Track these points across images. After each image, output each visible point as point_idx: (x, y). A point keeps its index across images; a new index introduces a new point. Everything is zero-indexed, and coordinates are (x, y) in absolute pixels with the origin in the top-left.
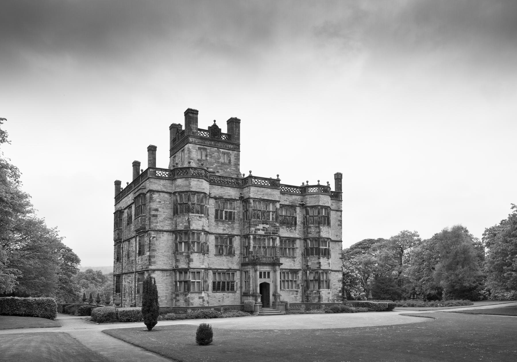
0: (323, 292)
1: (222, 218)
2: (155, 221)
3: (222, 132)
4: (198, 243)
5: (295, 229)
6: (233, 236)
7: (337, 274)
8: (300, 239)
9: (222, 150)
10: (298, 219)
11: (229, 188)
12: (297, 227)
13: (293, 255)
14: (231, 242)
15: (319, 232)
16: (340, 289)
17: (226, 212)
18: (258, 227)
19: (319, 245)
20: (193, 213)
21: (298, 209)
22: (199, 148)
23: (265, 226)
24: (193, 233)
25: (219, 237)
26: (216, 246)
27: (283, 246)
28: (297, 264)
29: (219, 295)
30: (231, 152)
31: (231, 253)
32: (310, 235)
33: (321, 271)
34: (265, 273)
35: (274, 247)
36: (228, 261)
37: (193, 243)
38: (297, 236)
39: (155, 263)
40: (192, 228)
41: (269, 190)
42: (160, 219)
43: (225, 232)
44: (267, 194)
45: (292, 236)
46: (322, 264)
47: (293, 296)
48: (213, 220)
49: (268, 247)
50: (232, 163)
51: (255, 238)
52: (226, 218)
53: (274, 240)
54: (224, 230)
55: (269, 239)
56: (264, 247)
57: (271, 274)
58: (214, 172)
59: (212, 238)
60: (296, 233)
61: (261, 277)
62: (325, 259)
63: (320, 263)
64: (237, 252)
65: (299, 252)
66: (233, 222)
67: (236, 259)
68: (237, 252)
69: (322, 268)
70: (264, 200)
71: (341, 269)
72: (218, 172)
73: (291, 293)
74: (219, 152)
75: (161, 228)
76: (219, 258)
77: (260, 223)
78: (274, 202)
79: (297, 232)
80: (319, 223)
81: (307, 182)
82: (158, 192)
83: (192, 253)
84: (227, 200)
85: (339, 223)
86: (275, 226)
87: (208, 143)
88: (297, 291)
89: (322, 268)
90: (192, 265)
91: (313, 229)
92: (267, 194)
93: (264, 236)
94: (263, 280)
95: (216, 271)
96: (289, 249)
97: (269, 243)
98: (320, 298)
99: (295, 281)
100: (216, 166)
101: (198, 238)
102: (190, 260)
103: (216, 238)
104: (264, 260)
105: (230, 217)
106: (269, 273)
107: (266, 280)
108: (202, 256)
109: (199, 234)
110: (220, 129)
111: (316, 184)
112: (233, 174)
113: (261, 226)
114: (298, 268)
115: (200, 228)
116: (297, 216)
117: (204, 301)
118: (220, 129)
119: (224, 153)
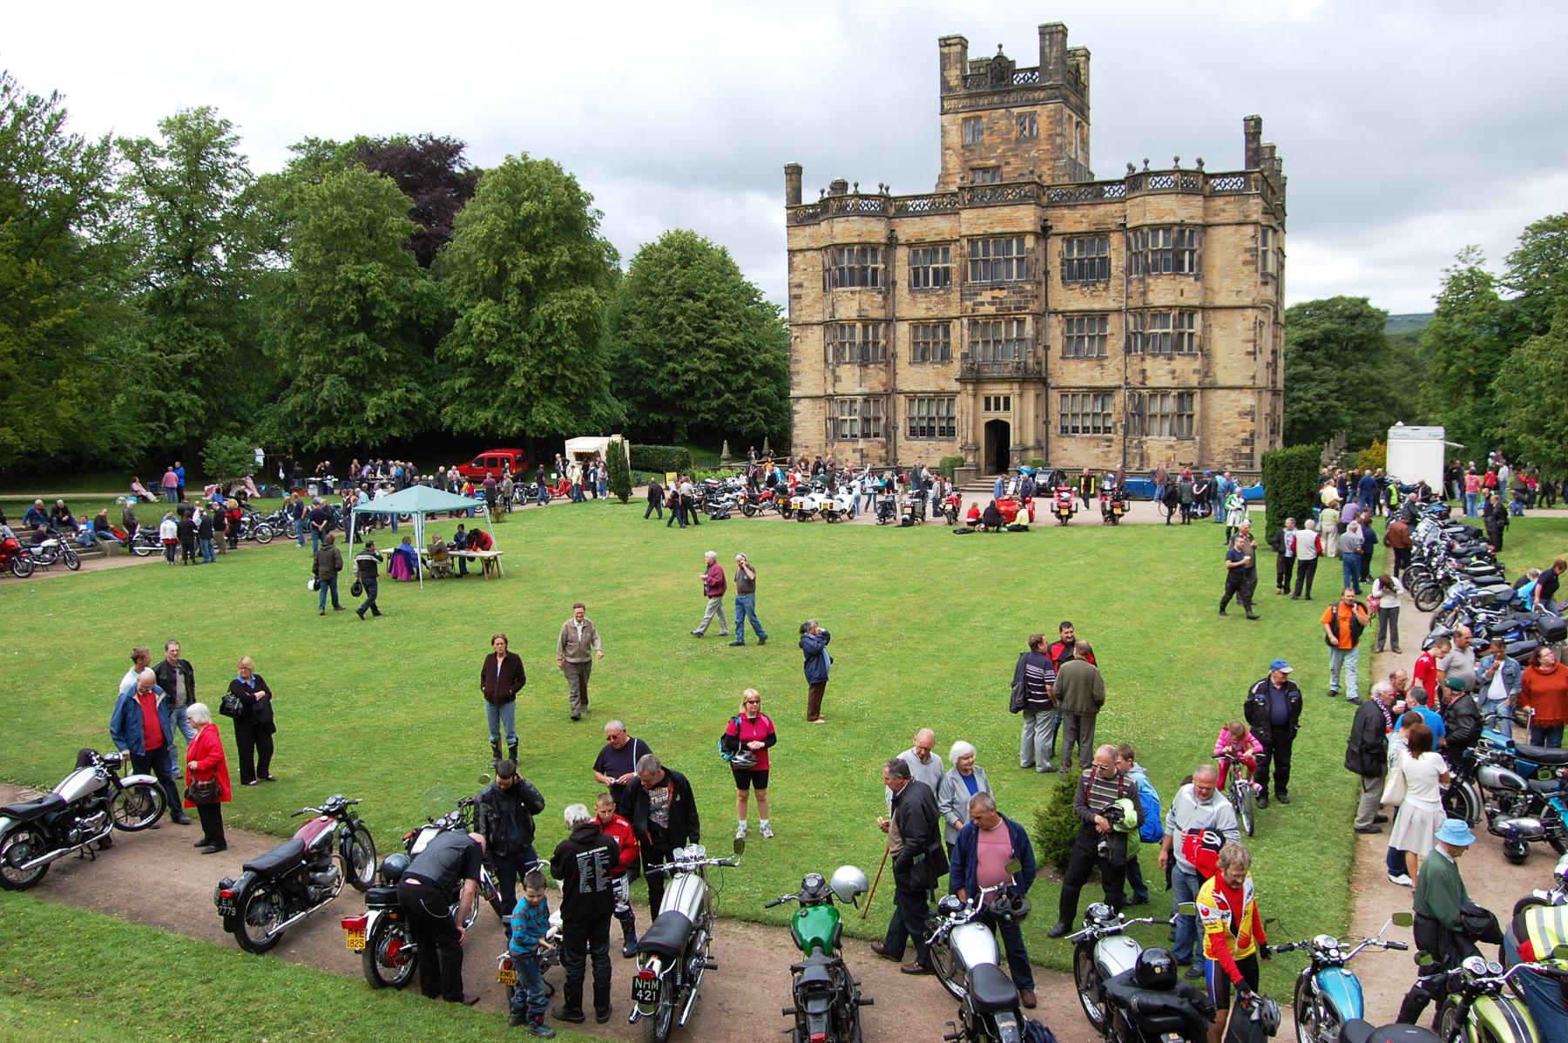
0: (1150, 443)
1: (926, 283)
2: (797, 307)
3: (1018, 67)
4: (852, 344)
5: (1106, 289)
6: (950, 319)
7: (1234, 395)
8: (1119, 311)
9: (1016, 111)
10: (1113, 263)
11: (937, 218)
12: (1112, 283)
13: (1101, 350)
14: (947, 333)
15: (1144, 294)
16: (1246, 435)
17: (936, 271)
18: (979, 299)
19: (1143, 327)
20: (842, 285)
21: (1116, 240)
22: (965, 120)
23: (996, 293)
24: (842, 327)
25: (917, 325)
26: (916, 344)
27: (1075, 333)
28: (1109, 376)
29: (920, 444)
30: (1038, 109)
31: (946, 357)
32: (1131, 303)
33: (1144, 392)
34: (997, 400)
35: (1021, 340)
36: (937, 374)
37: (843, 344)
38: (1112, 305)
39: (799, 384)
40: (837, 317)
41: (1006, 210)
42: (806, 301)
43: (930, 314)
44: (1001, 221)
45: (1097, 306)
46: (1148, 373)
47: (1098, 451)
48: (906, 291)
49: (1008, 341)
50: (1042, 137)
51: (974, 323)
52: (935, 284)
53: (1021, 322)
54: (928, 309)
55: (1010, 322)
56: (998, 342)
57: (1014, 402)
58: (999, 167)
59: (903, 330)
60: (1107, 299)
61: (988, 408)
62: (1161, 360)
63: (1144, 371)
64: (957, 355)
65: (1115, 344)
66: (948, 291)
67: (956, 368)
68: (957, 355)
69: (1149, 383)
70: (993, 235)
71: (1250, 383)
72: (1007, 164)
73: (1093, 443)
74: (1009, 117)
75: (808, 319)
76: (918, 368)
77: (984, 288)
78: (1020, 236)
79: (1112, 293)
80: (1147, 271)
81: (1146, 162)
82: (801, 250)
83: (838, 364)
84: (935, 244)
85: (1248, 257)
86: (1021, 292)
87: (985, 101)
88: (1110, 440)
89: (1149, 383)
90: (840, 389)
91: (1135, 287)
92: (1001, 221)
93: (995, 316)
94: (993, 415)
95: (912, 397)
96: (1092, 338)
97: (1008, 331)
98: (1143, 458)
99: (1109, 415)
100: (1004, 152)
101: (852, 335)
102: (837, 379)
103: (916, 327)
104: (996, 372)
105: (943, 277)
106: (1007, 400)
107: (1001, 415)
108: (857, 370)
109: (853, 327)
110: (1013, 62)
111: (1170, 166)
112: (1044, 162)
113: (986, 296)
114: (1112, 384)
115: (854, 315)
116: (1113, 256)
117: (862, 456)
118: (1013, 62)
119: (1020, 116)
